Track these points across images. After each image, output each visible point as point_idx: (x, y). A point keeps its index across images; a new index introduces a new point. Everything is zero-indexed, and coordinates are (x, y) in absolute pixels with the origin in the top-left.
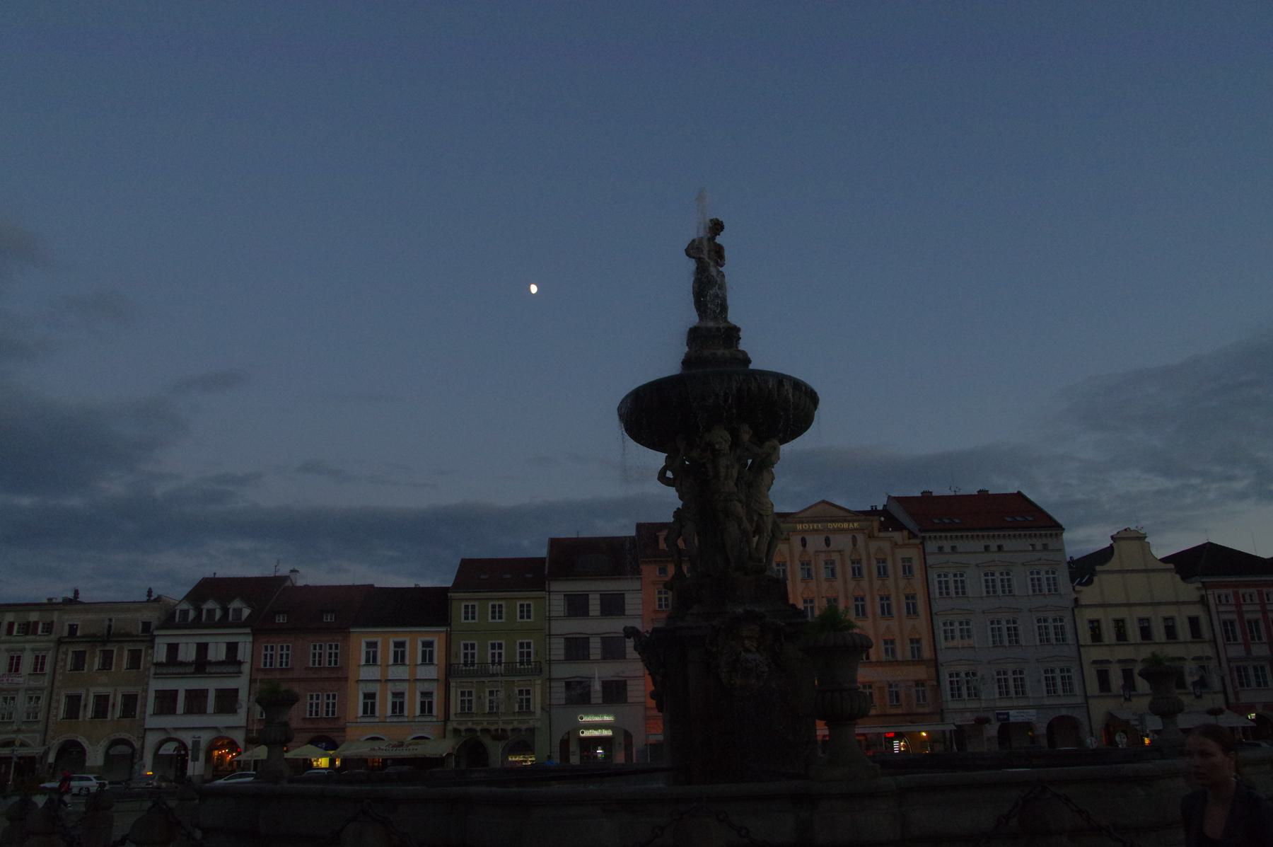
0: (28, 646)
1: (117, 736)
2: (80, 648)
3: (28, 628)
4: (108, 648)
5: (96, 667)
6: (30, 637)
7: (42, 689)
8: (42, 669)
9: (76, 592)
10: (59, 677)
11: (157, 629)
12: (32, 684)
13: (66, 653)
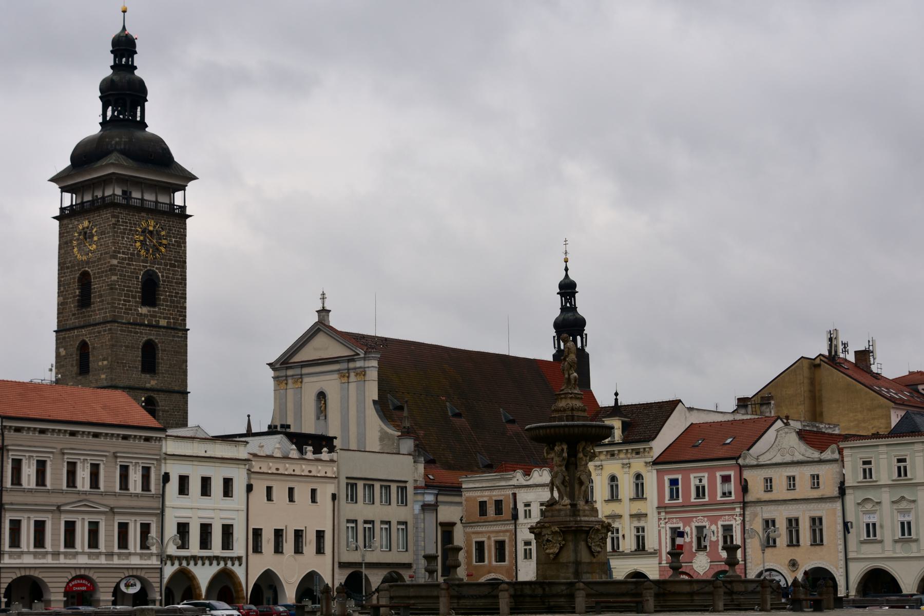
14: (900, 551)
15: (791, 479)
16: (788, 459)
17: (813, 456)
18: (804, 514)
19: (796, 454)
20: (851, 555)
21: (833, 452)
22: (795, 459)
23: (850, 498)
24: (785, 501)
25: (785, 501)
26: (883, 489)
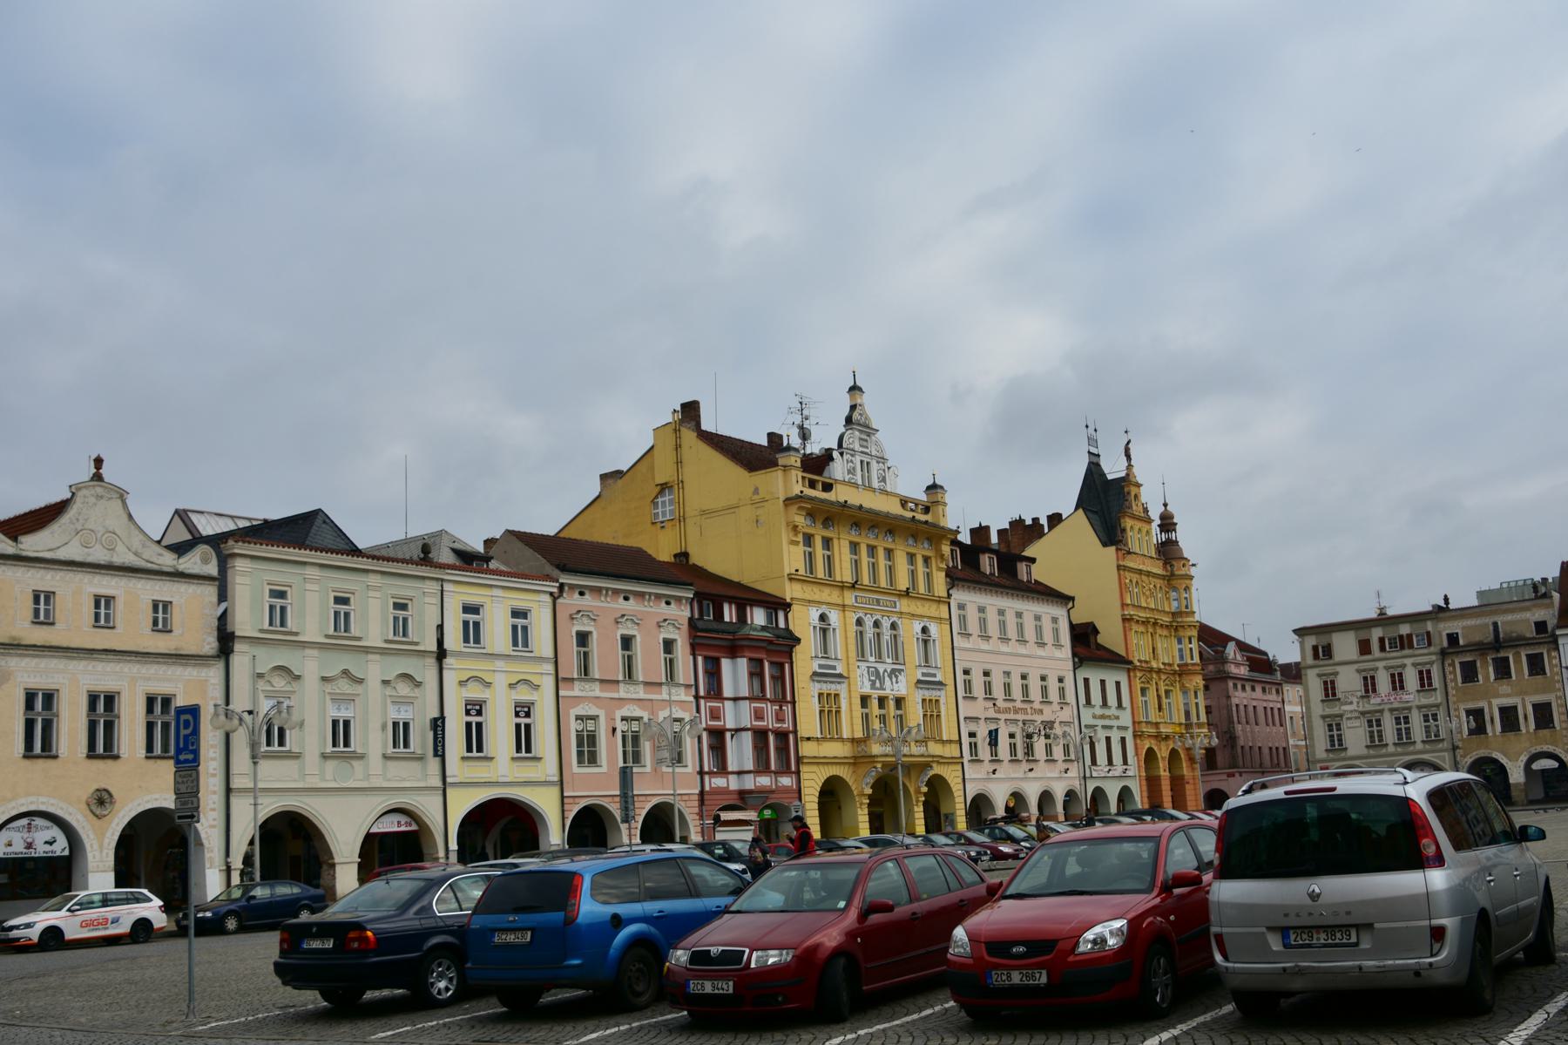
0: (1408, 661)
1: (1539, 749)
2: (1468, 658)
3: (1404, 643)
4: (1502, 654)
5: (1492, 677)
6: (1407, 652)
7: (1437, 706)
8: (1430, 684)
9: (1446, 599)
10: (1452, 692)
11: (1559, 627)
12: (1424, 701)
13: (1453, 665)
14: (331, 774)
15: (103, 603)
16: (98, 555)
17: (160, 561)
18: (133, 687)
19: (120, 548)
20: (236, 783)
21: (205, 561)
22: (117, 560)
23: (241, 659)
24: (90, 653)
25: (90, 653)
26: (308, 652)
